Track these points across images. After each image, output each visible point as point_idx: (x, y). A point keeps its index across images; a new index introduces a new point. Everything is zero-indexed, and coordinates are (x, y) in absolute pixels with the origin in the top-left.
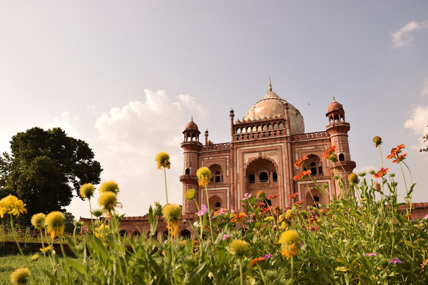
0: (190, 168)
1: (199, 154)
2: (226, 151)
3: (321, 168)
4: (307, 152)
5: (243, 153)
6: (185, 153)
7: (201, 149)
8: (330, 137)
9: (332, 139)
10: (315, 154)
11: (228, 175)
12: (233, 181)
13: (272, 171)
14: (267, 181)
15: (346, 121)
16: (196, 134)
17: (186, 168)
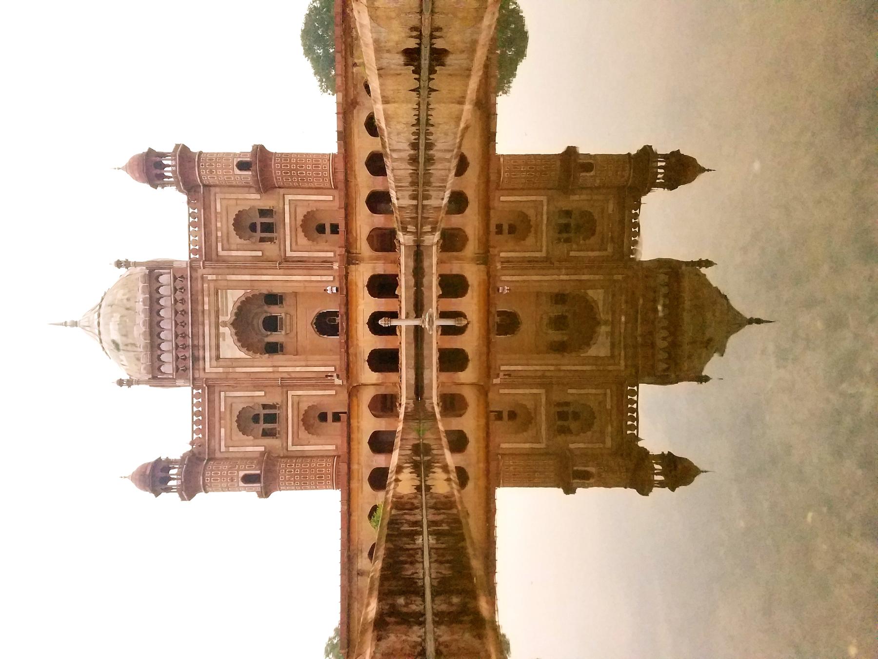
0: (242, 474)
1: (210, 459)
3: (263, 213)
5: (218, 358)
7: (200, 453)
11: (262, 393)
12: (276, 379)
13: (260, 306)
15: (171, 150)
17: (241, 484)
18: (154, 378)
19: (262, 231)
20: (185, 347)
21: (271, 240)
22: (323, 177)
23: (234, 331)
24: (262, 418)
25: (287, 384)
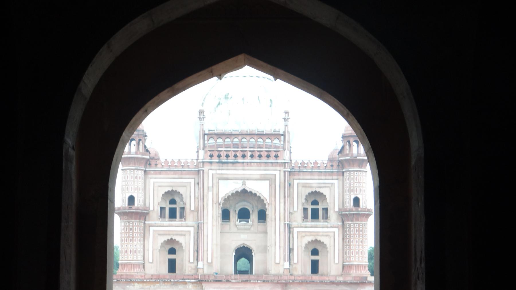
0: (135, 195)
1: (145, 171)
2: (190, 172)
3: (326, 210)
4: (311, 187)
5: (219, 179)
6: (125, 169)
7: (150, 164)
8: (344, 170)
9: (345, 174)
10: (321, 190)
11: (192, 208)
13: (257, 206)
14: (248, 222)
16: (143, 139)
17: (128, 195)
18: (205, 134)
19: (312, 209)
20: (227, 156)
21: (305, 217)
22: (350, 257)
23: (239, 190)
24: (173, 206)
25: (199, 229)
